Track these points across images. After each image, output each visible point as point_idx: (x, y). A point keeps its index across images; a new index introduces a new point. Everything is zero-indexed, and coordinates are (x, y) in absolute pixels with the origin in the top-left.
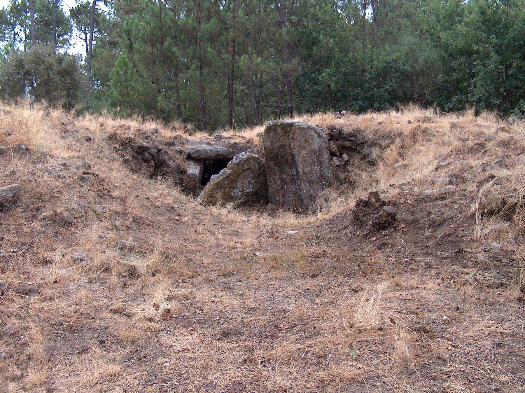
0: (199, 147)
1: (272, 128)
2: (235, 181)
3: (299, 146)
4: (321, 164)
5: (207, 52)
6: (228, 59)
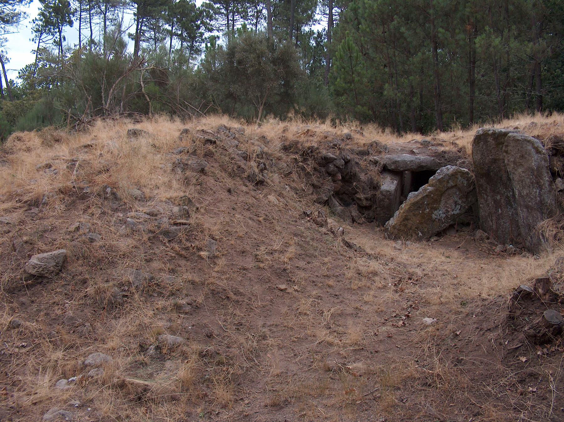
0: (399, 157)
1: (482, 137)
2: (437, 201)
3: (515, 163)
4: (540, 187)
5: (438, 32)
6: (464, 40)
